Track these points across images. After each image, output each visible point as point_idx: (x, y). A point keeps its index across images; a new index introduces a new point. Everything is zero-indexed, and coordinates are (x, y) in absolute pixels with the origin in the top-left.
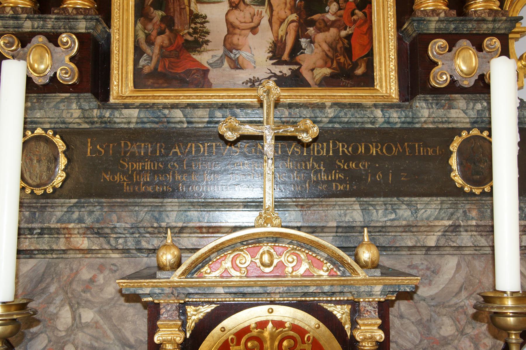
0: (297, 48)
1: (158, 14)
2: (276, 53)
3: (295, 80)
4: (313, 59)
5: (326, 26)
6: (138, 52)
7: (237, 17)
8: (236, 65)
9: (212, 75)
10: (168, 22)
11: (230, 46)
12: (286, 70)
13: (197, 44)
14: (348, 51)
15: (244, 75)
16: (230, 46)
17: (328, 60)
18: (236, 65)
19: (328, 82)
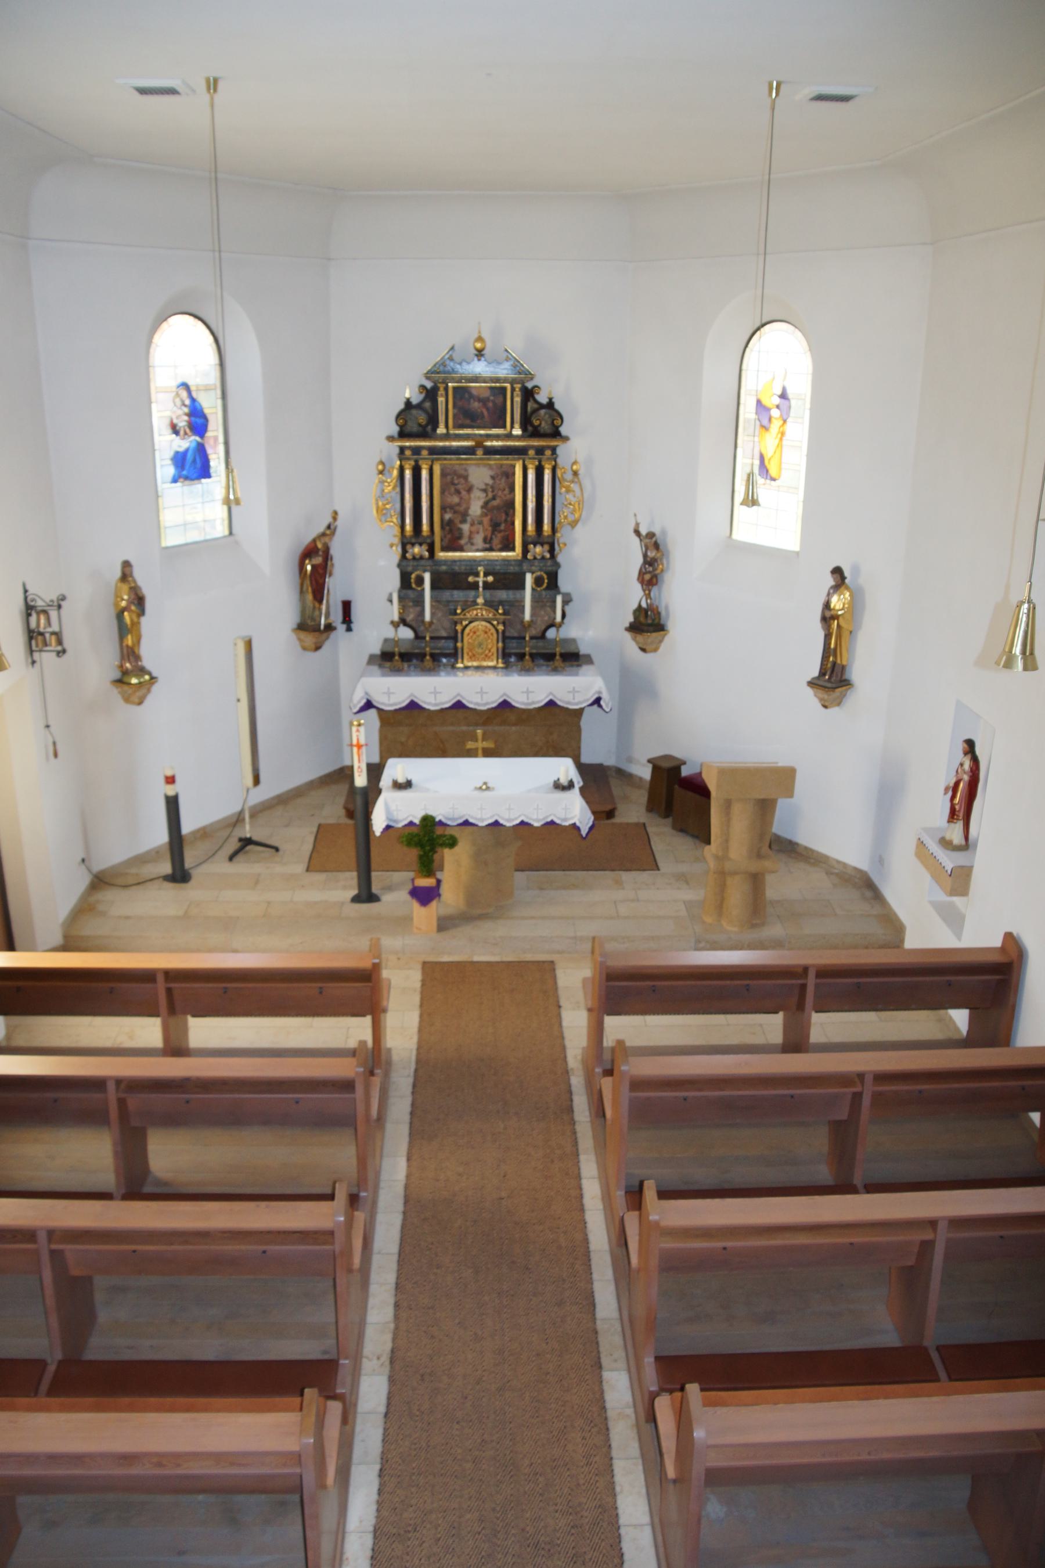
0: (491, 539)
1: (447, 528)
2: (485, 540)
3: (491, 549)
4: (496, 542)
5: (500, 531)
6: (442, 540)
7: (474, 529)
8: (472, 544)
9: (465, 548)
10: (451, 531)
11: (470, 538)
12: (487, 546)
13: (460, 537)
14: (507, 540)
15: (474, 548)
16: (470, 538)
17: (501, 542)
18: (472, 544)
19: (502, 550)
